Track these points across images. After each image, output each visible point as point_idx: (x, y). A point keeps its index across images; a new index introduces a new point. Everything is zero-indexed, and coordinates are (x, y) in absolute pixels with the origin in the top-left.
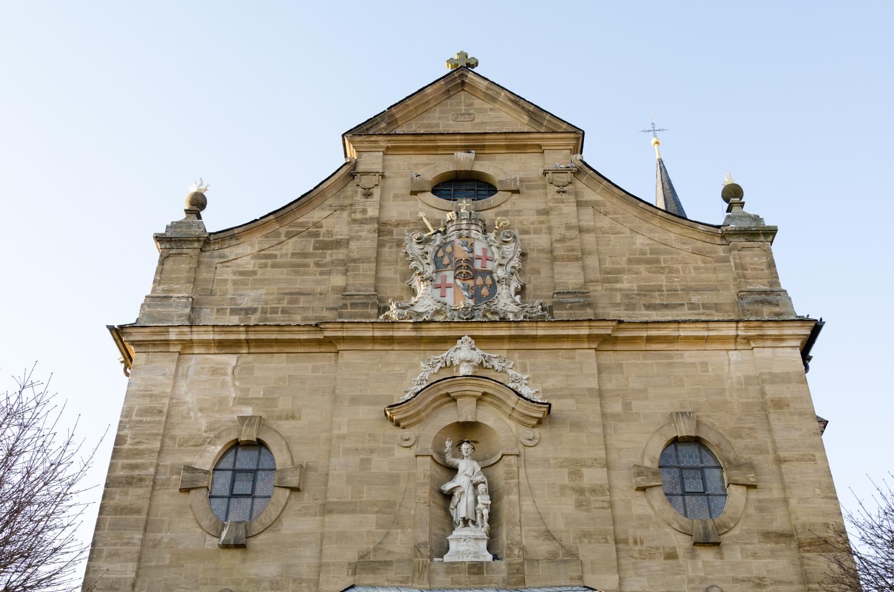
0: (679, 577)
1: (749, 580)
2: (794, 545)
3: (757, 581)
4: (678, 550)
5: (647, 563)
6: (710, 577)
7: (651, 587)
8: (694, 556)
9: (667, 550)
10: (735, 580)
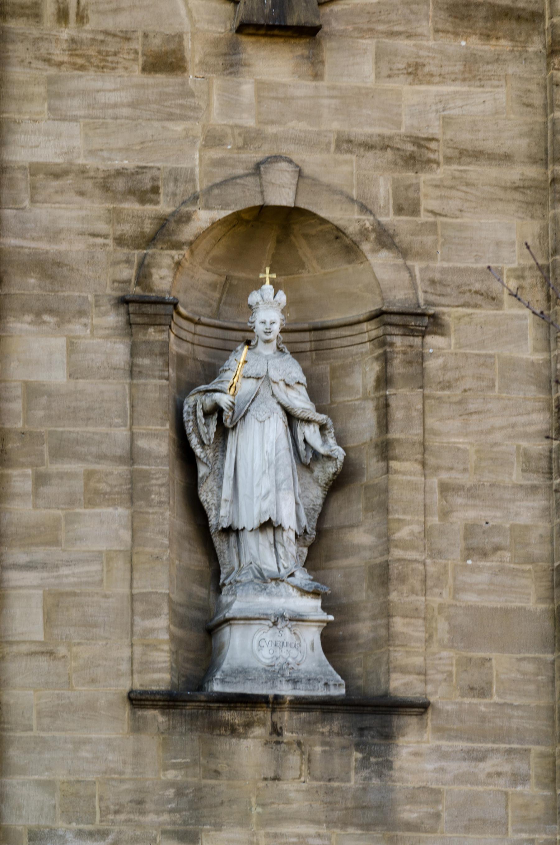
0: (178, 128)
1: (383, 145)
2: (537, 45)
3: (410, 147)
4: (188, 44)
5: (90, 80)
6: (271, 130)
7: (92, 153)
8: (230, 62)
9: (156, 43)
10: (345, 143)
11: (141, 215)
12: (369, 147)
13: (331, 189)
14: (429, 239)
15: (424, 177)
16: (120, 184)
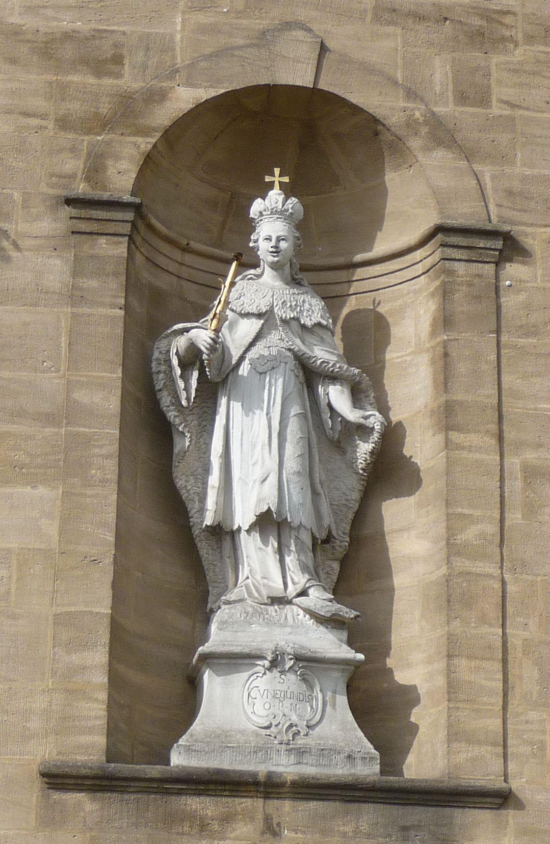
3: (477, 22)
11: (93, 90)
12: (419, 17)
13: (368, 69)
14: (504, 138)
15: (496, 59)
16: (68, 51)
